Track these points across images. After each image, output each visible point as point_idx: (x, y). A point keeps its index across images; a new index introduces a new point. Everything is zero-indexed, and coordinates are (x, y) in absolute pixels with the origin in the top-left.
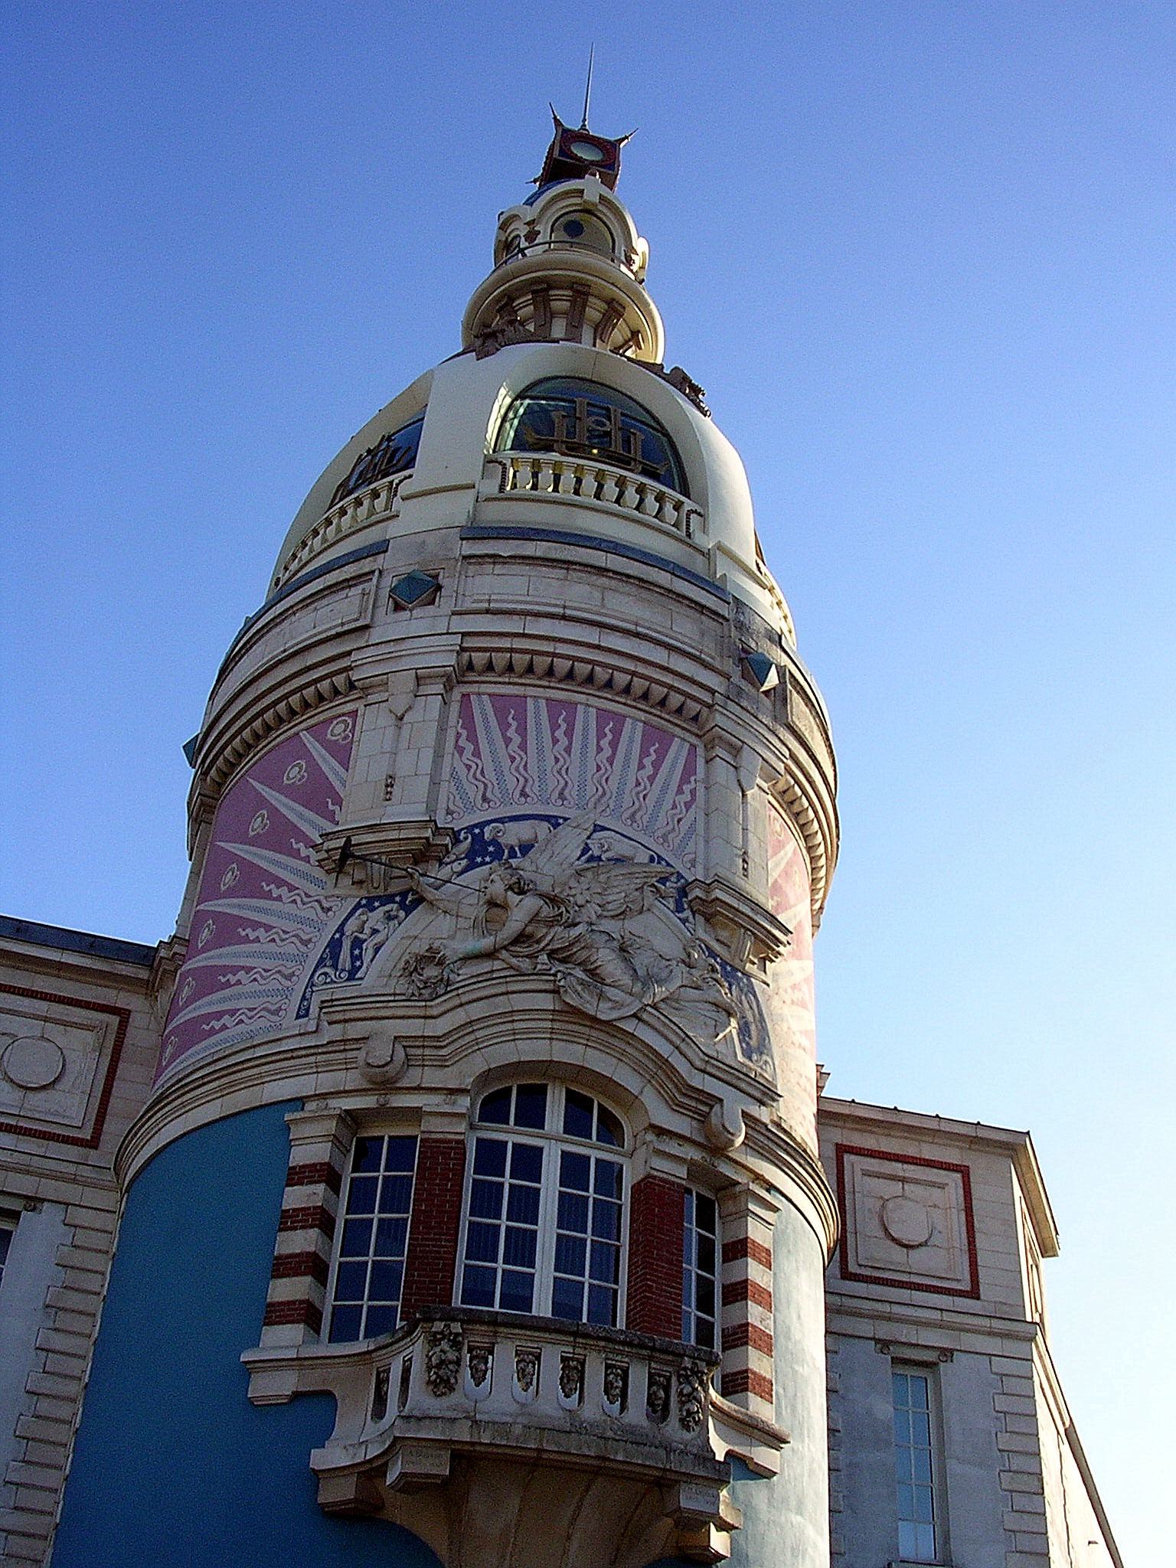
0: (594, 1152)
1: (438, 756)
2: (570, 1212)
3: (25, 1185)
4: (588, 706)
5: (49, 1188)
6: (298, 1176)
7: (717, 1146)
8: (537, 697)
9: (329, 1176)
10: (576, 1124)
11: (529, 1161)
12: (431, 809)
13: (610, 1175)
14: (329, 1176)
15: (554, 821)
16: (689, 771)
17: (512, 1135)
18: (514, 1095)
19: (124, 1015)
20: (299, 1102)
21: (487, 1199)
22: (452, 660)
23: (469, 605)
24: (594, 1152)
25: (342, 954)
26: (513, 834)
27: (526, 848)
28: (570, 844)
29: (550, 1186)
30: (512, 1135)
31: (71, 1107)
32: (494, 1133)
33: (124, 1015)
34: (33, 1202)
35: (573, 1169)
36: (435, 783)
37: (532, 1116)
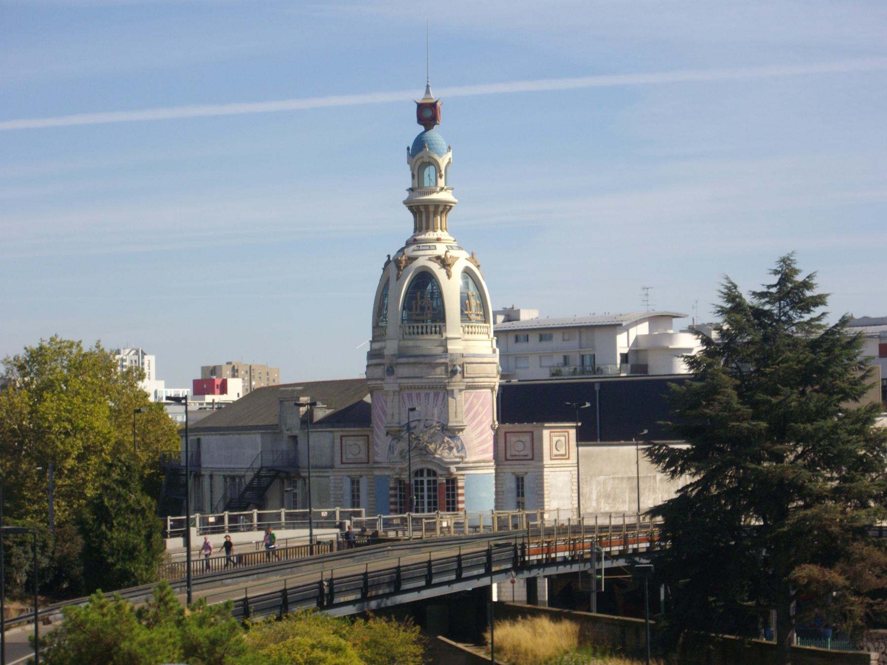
0: (431, 478)
1: (399, 408)
2: (429, 490)
3: (359, 473)
4: (423, 393)
5: (363, 473)
6: (391, 489)
7: (451, 474)
8: (414, 393)
9: (395, 489)
10: (429, 475)
11: (422, 482)
12: (400, 419)
13: (435, 482)
14: (395, 489)
15: (419, 421)
16: (444, 398)
17: (419, 479)
18: (420, 473)
19: (368, 436)
20: (389, 476)
21: (417, 490)
22: (397, 389)
23: (400, 376)
24: (431, 478)
25: (391, 449)
26: (412, 425)
27: (415, 427)
28: (422, 424)
29: (425, 486)
30: (419, 479)
31: (363, 456)
32: (417, 479)
33: (368, 436)
34: (361, 476)
35: (429, 482)
36: (399, 414)
37: (422, 475)
